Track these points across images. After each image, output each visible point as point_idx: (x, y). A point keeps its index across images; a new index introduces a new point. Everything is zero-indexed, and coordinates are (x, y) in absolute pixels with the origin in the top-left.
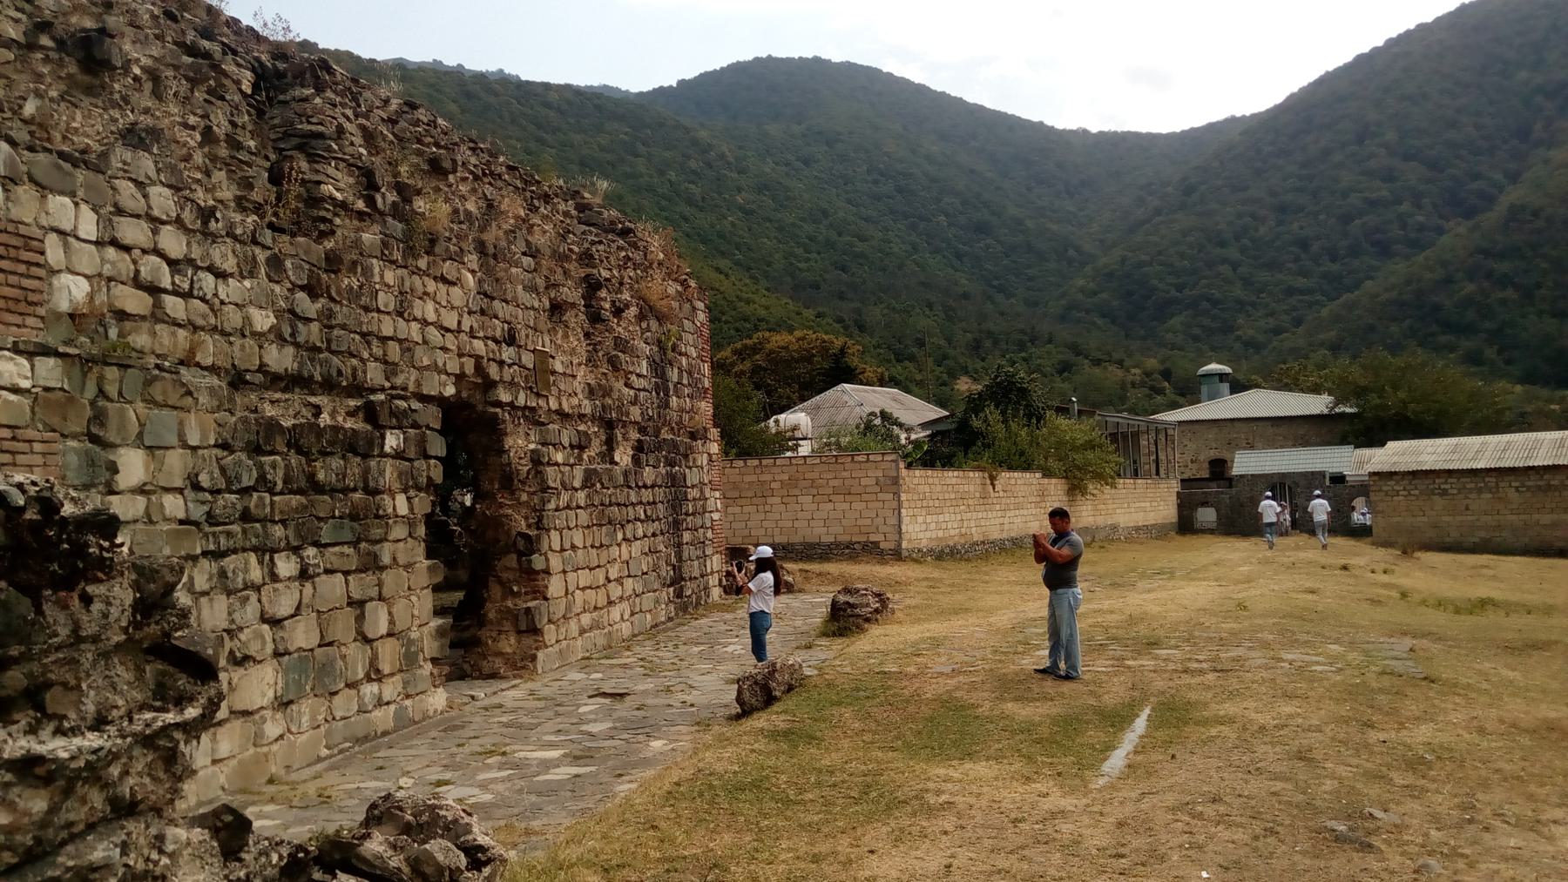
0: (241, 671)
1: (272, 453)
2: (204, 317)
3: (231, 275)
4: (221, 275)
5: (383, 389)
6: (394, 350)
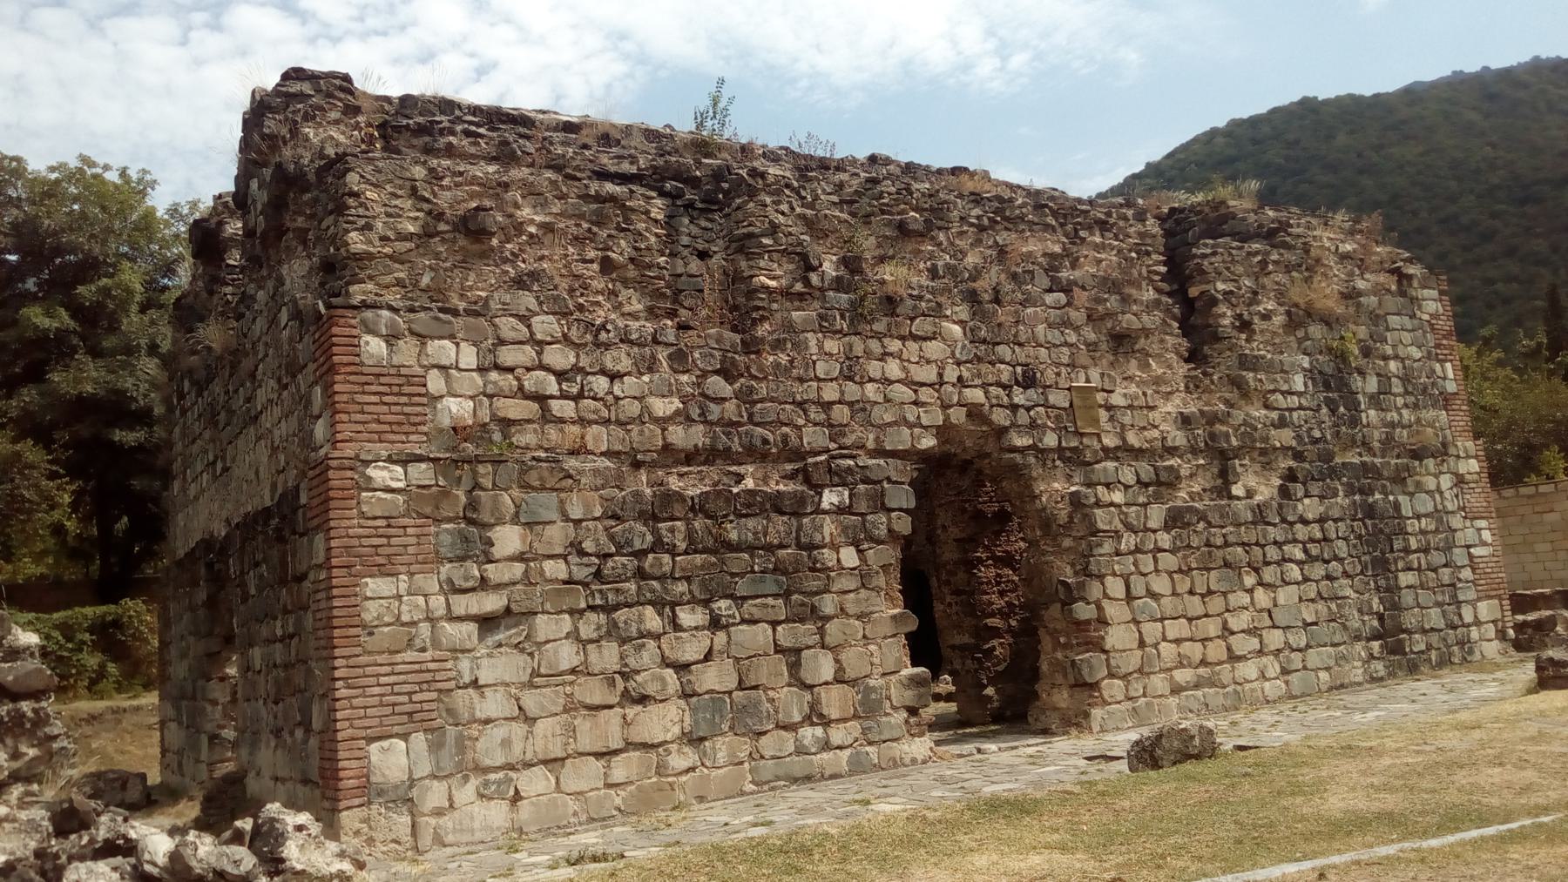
0: (640, 708)
1: (672, 519)
2: (596, 412)
3: (628, 374)
4: (614, 377)
5: (827, 451)
6: (841, 414)
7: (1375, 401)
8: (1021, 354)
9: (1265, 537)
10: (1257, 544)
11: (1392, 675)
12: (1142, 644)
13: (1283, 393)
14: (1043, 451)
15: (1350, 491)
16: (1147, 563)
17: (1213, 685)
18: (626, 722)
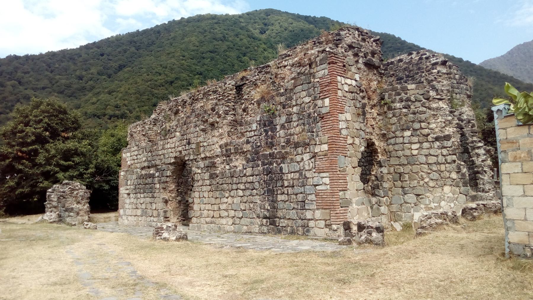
8: (189, 136)
11: (269, 232)
12: (200, 210)
13: (249, 132)
14: (192, 160)
15: (263, 164)
16: (204, 188)
17: (215, 223)
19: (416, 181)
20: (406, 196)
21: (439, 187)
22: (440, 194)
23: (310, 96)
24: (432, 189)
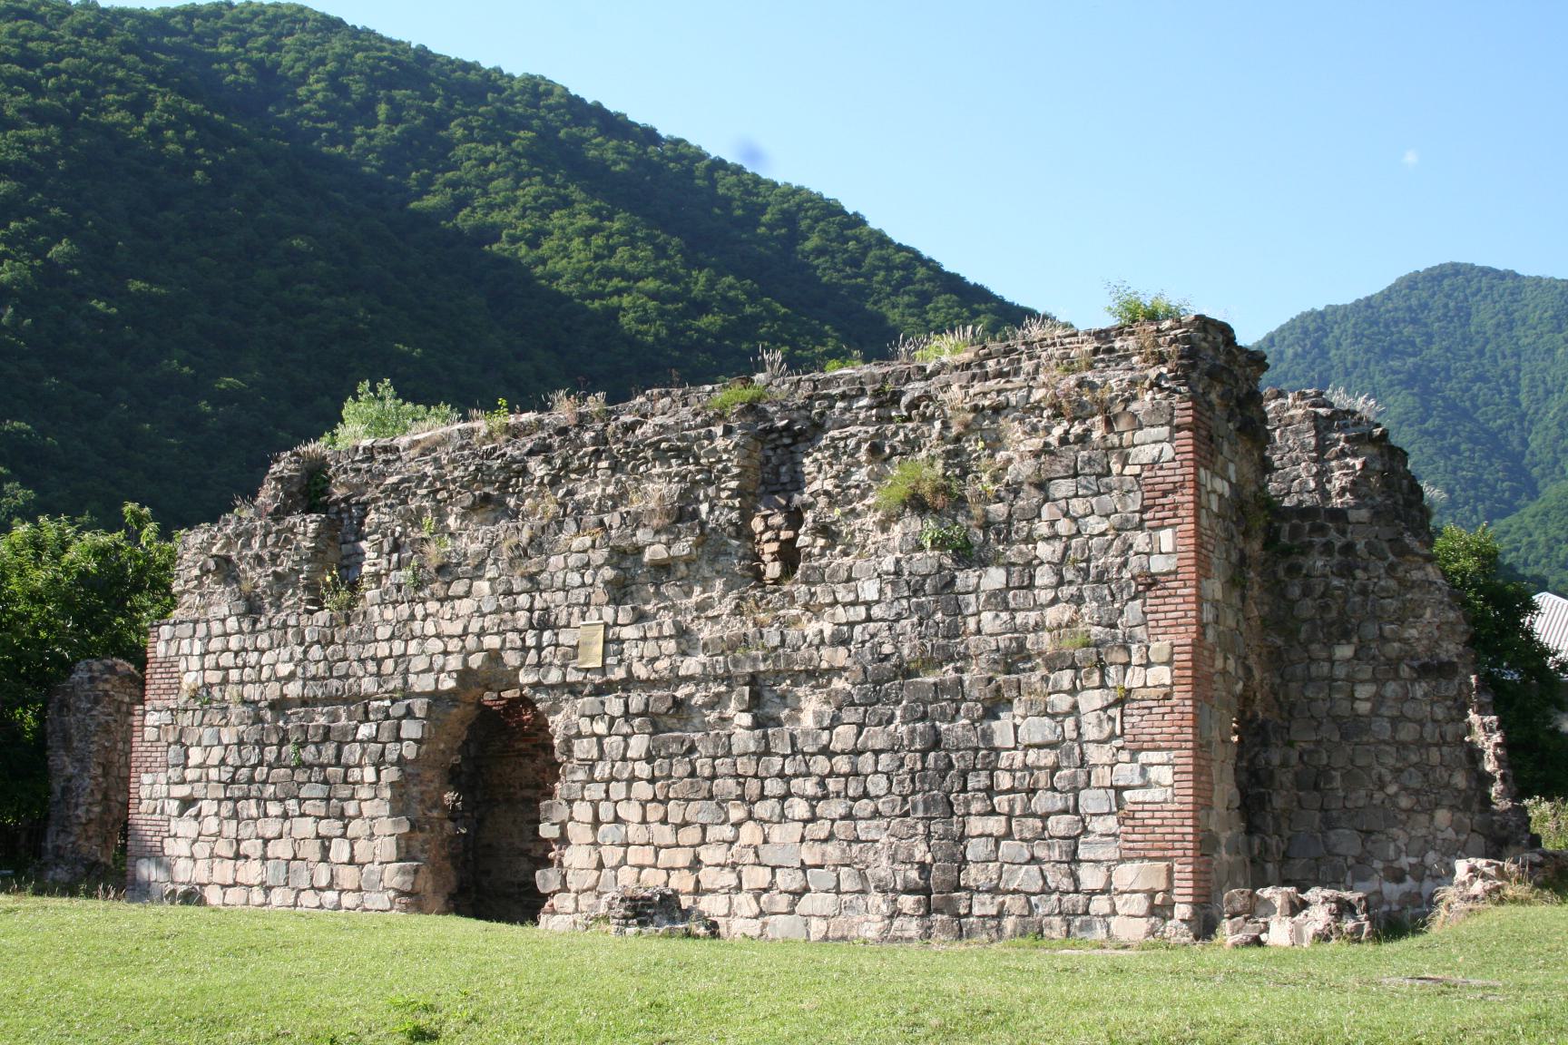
7: (998, 600)
9: (767, 769)
10: (756, 776)
18: (236, 871)
19: (1363, 793)
20: (1331, 833)
21: (1424, 811)
22: (1423, 832)
23: (1108, 516)
24: (1403, 817)
